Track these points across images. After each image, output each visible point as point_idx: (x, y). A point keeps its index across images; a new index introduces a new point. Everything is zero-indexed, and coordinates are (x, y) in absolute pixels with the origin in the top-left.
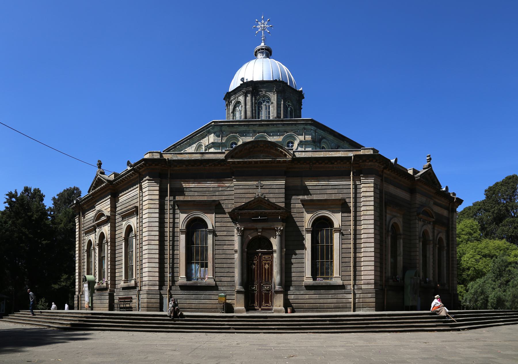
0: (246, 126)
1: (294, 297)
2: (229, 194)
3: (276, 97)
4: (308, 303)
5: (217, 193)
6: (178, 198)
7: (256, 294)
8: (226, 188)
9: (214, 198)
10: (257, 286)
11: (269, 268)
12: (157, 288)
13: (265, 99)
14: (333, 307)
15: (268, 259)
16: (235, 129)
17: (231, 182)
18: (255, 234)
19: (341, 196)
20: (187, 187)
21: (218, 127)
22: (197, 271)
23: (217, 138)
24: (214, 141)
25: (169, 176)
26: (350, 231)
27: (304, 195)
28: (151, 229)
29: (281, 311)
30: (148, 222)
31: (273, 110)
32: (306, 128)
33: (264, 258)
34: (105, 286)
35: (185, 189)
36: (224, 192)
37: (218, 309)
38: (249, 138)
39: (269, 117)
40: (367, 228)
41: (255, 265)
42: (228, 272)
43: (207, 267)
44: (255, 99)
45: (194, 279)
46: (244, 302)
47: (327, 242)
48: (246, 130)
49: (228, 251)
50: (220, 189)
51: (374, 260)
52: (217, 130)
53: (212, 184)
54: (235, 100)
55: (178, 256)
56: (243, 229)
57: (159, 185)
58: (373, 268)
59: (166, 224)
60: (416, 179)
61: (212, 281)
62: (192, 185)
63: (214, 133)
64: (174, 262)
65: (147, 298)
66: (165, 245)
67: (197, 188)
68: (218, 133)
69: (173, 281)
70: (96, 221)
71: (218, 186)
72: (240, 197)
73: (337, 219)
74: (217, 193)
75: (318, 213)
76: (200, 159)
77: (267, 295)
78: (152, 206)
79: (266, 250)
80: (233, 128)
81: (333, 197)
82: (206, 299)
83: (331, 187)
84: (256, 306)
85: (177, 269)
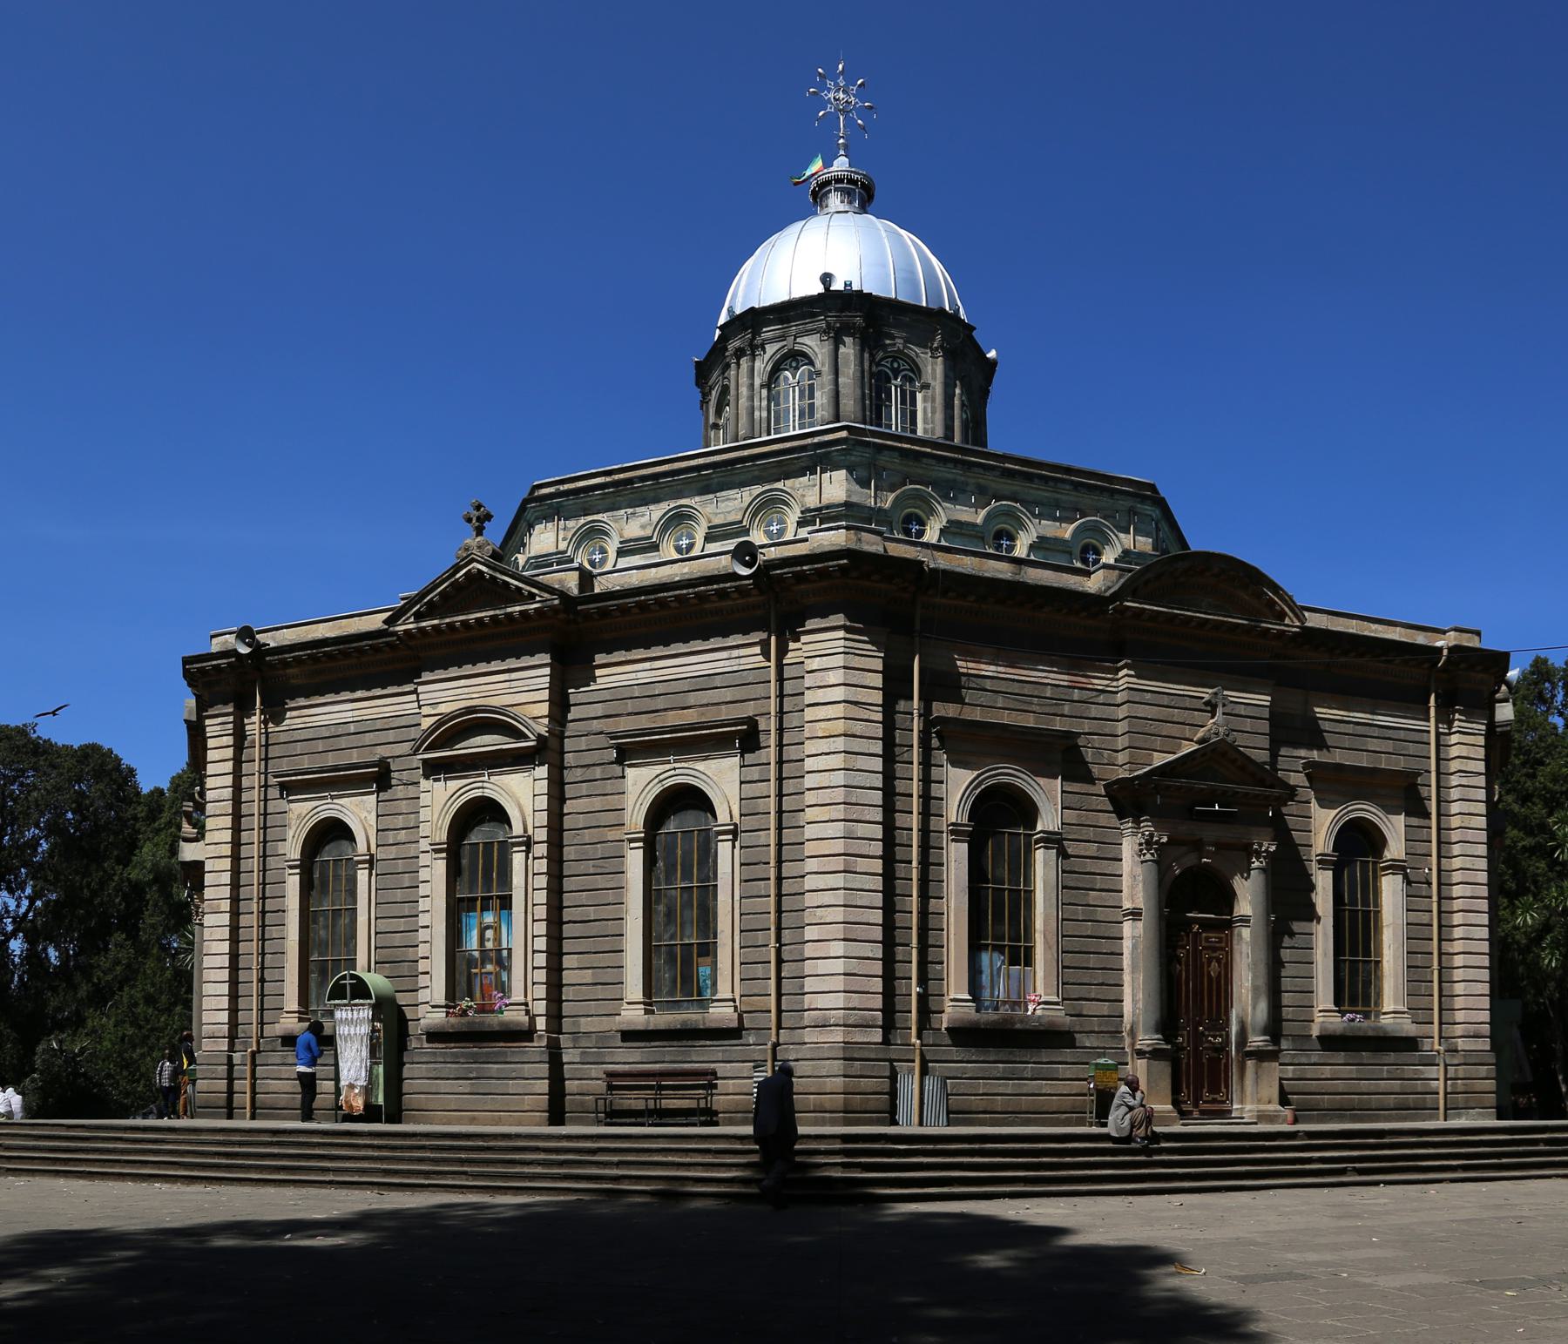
0: (959, 466)
1: (1294, 1070)
2: (1104, 717)
3: (939, 369)
4: (1329, 1091)
5: (1067, 709)
6: (940, 709)
7: (1185, 1061)
8: (1095, 693)
9: (1058, 725)
10: (1185, 1032)
11: (1220, 973)
12: (877, 1036)
13: (899, 366)
14: (1392, 1106)
15: (1217, 945)
16: (922, 468)
17: (1109, 676)
18: (1190, 860)
19: (1402, 763)
20: (970, 671)
21: (868, 450)
22: (995, 978)
23: (857, 487)
24: (848, 496)
25: (918, 626)
26: (1427, 871)
27: (1310, 747)
28: (855, 813)
29: (1276, 1116)
30: (845, 786)
31: (929, 410)
32: (1139, 510)
33: (1207, 939)
34: (523, 1024)
35: (964, 679)
36: (1088, 708)
37: (1085, 1113)
38: (965, 508)
39: (914, 431)
40: (1471, 867)
41: (1180, 965)
42: (1102, 984)
43: (1029, 961)
44: (870, 360)
45: (987, 1004)
46: (1170, 1087)
47: (1366, 903)
48: (955, 480)
49: (1101, 911)
50: (1076, 694)
51: (1488, 965)
52: (858, 459)
53: (1052, 675)
54: (785, 343)
55: (942, 922)
56: (1165, 839)
57: (882, 655)
58: (1485, 988)
59: (898, 797)
60: (1500, 732)
61: (1058, 1013)
62: (989, 670)
63: (850, 471)
64: (927, 941)
65: (845, 1076)
66: (897, 876)
67: (1003, 682)
68: (863, 473)
69: (926, 1012)
70: (430, 748)
71: (1070, 684)
72: (1146, 730)
73: (1395, 830)
74: (1067, 709)
75: (1349, 808)
76: (1011, 579)
77: (1214, 1062)
78: (858, 728)
79: (1213, 916)
80: (916, 464)
81: (1384, 763)
82: (1041, 1076)
83: (1376, 732)
84: (1185, 1102)
85: (938, 967)
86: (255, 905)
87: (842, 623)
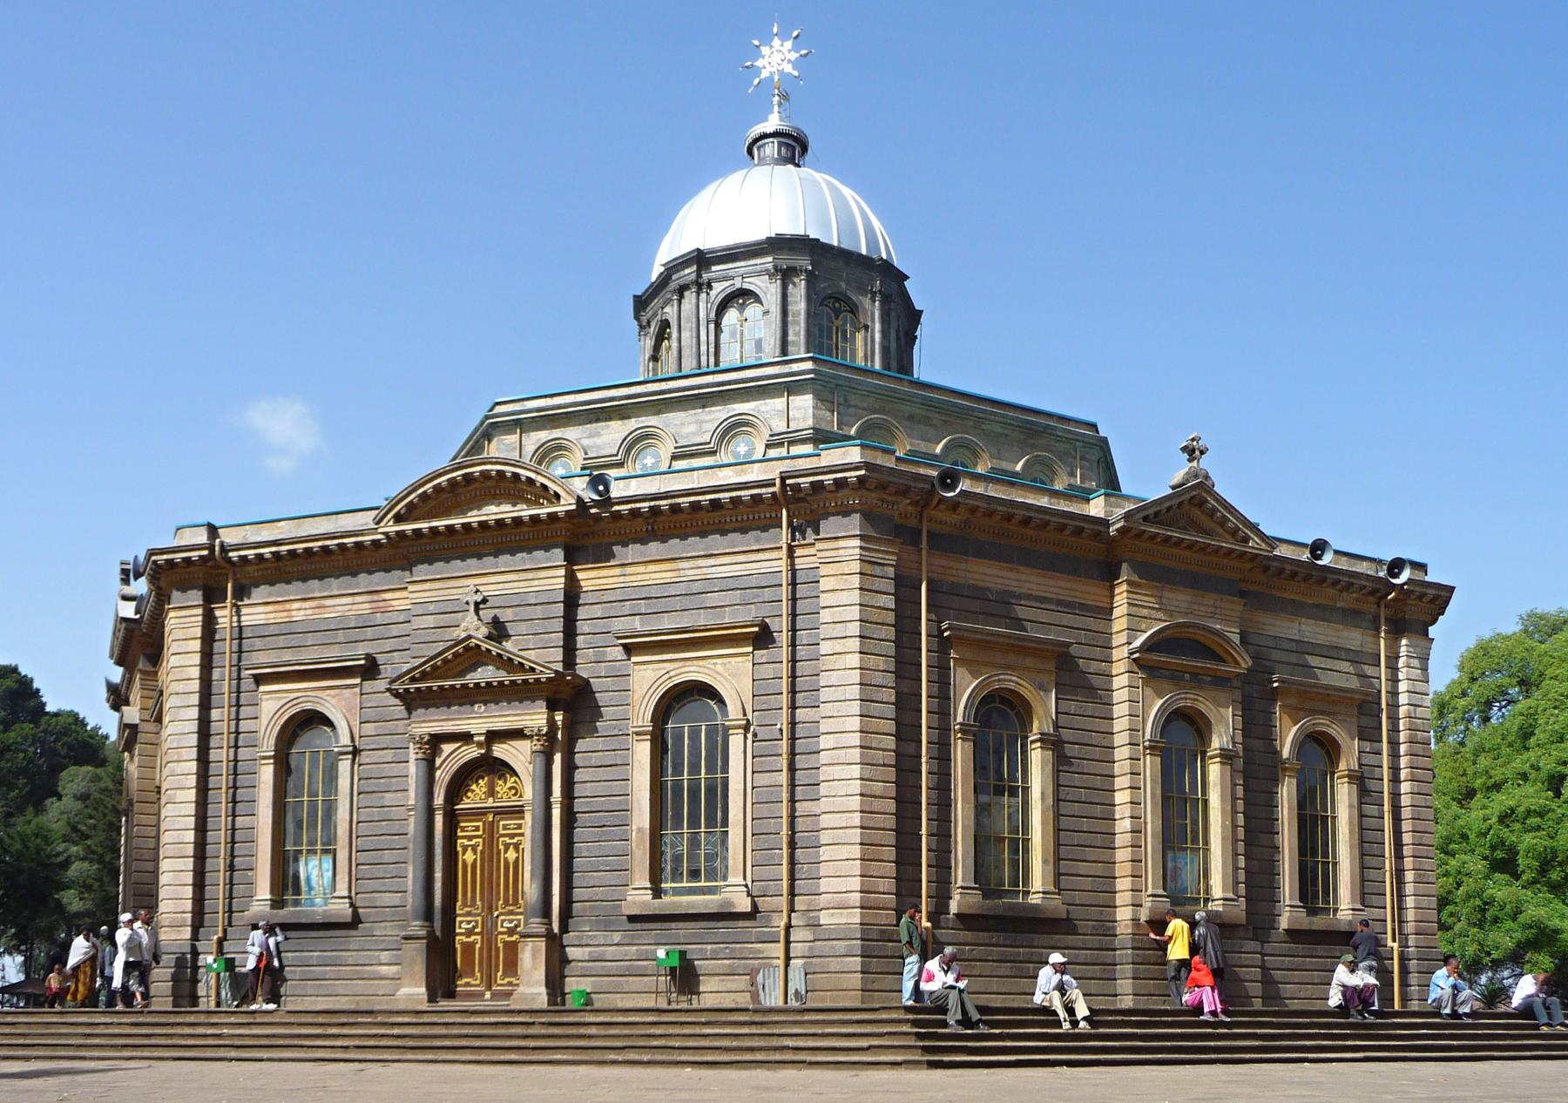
46: (424, 971)
86: (224, 795)
87: (858, 533)
